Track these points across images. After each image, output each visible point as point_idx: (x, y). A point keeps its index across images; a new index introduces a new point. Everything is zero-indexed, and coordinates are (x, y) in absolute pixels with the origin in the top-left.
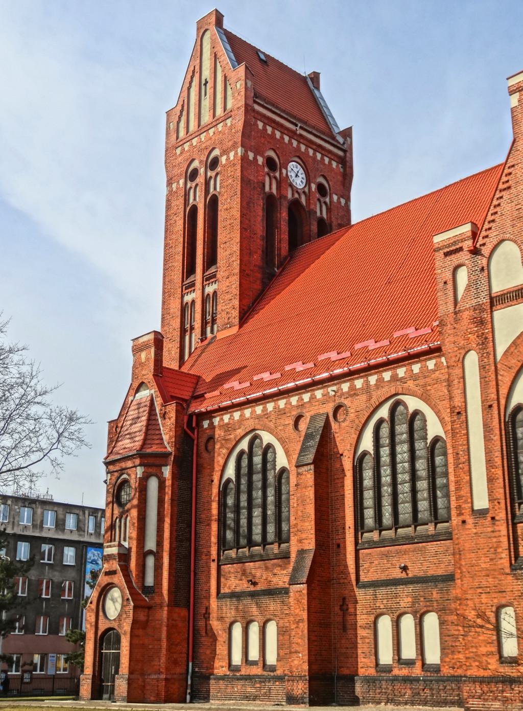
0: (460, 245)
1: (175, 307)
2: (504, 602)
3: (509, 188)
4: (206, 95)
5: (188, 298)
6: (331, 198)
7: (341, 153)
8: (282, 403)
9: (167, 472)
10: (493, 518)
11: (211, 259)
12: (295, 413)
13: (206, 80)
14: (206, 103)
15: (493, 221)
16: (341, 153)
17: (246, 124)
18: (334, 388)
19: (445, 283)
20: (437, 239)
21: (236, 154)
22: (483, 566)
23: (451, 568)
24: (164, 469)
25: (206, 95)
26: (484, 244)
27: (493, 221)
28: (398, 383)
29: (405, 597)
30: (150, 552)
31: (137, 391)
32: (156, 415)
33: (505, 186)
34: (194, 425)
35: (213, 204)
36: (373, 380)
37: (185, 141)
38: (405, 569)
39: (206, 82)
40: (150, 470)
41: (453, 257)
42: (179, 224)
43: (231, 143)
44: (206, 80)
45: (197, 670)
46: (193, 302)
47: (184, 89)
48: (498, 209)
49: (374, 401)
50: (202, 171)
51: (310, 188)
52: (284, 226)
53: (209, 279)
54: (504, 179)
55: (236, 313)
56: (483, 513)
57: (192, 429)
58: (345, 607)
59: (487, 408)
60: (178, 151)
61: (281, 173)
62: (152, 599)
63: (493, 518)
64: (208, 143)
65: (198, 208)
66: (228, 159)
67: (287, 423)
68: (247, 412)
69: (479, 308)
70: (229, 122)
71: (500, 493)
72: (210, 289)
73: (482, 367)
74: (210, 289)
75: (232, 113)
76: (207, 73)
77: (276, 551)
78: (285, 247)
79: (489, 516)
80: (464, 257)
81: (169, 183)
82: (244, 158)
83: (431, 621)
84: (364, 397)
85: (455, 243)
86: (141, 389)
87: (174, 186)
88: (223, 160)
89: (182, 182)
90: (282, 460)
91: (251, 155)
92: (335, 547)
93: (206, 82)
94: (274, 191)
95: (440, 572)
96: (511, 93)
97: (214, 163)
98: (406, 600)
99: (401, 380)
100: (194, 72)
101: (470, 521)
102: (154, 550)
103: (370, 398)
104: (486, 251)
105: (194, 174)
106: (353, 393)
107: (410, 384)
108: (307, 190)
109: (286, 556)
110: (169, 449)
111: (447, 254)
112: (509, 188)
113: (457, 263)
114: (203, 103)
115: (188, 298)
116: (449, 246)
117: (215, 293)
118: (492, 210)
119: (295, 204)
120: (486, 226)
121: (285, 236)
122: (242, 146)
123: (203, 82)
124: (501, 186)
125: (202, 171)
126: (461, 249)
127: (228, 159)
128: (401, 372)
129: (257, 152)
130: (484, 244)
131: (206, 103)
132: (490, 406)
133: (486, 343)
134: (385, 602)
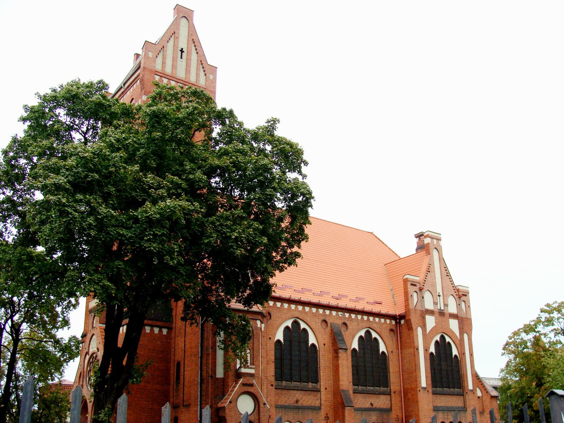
0: (415, 284)
4: (181, 58)
8: (314, 310)
10: (428, 391)
13: (182, 49)
14: (181, 64)
18: (342, 313)
25: (181, 58)
28: (370, 323)
33: (428, 270)
36: (359, 317)
44: (182, 49)
56: (424, 389)
59: (426, 350)
67: (317, 321)
68: (293, 307)
69: (422, 311)
71: (430, 382)
77: (310, 387)
79: (427, 390)
85: (414, 282)
95: (385, 407)
99: (371, 322)
103: (358, 325)
107: (375, 325)
109: (319, 391)
111: (412, 284)
126: (415, 285)
128: (371, 319)
133: (424, 327)
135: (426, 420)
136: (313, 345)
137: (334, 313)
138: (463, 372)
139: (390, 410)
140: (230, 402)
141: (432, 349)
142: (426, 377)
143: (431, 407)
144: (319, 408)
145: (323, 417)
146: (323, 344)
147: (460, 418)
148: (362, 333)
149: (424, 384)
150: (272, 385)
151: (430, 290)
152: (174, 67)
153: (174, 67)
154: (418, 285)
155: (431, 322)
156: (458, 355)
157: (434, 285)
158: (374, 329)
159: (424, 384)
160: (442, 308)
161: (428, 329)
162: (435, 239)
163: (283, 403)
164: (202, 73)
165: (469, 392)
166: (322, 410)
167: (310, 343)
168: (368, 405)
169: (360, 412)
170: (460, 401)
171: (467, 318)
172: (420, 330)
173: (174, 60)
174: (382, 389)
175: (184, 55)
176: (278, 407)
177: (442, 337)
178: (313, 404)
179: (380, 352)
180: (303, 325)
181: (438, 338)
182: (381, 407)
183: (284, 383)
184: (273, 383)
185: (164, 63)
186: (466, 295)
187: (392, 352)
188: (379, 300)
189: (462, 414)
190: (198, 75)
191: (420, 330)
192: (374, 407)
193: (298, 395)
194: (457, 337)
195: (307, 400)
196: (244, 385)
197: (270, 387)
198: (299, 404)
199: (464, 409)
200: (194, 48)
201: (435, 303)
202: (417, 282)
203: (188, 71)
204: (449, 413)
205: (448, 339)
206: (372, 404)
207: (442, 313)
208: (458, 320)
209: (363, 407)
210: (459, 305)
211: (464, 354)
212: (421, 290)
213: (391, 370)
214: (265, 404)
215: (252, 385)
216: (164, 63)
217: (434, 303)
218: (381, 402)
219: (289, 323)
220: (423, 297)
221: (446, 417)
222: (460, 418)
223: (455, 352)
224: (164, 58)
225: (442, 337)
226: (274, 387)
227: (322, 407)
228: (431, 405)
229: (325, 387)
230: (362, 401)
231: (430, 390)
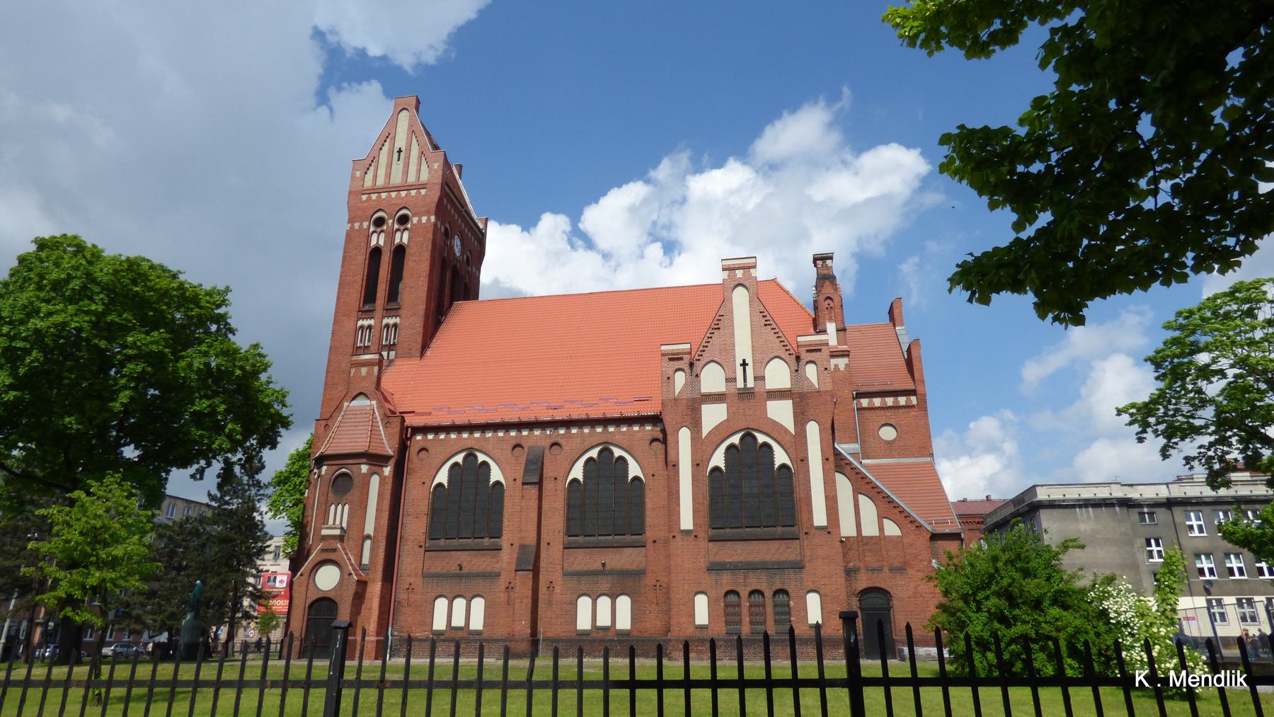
1: (349, 325)
2: (701, 590)
3: (719, 328)
4: (399, 160)
5: (366, 323)
6: (472, 269)
7: (481, 236)
9: (387, 471)
10: (696, 536)
11: (393, 295)
12: (514, 442)
14: (398, 168)
15: (706, 346)
16: (481, 236)
17: (440, 199)
19: (668, 378)
20: (663, 348)
21: (429, 219)
22: (687, 566)
23: (642, 566)
24: (384, 469)
25: (399, 160)
26: (699, 360)
27: (706, 346)
29: (605, 584)
30: (368, 537)
31: (354, 399)
32: (377, 422)
33: (716, 327)
34: (409, 436)
35: (400, 251)
37: (373, 191)
38: (604, 565)
39: (400, 151)
40: (373, 468)
41: (675, 362)
42: (360, 261)
43: (424, 209)
45: (395, 633)
46: (370, 327)
47: (375, 148)
48: (709, 340)
49: (587, 445)
50: (390, 221)
51: (463, 258)
52: (448, 283)
53: (392, 310)
54: (716, 322)
55: (419, 347)
56: (688, 532)
57: (408, 439)
58: (551, 588)
59: (697, 465)
60: (364, 197)
61: (451, 243)
62: (367, 574)
63: (696, 536)
64: (400, 201)
65: (383, 252)
66: (420, 221)
67: (504, 447)
70: (423, 192)
72: (391, 321)
73: (693, 439)
74: (391, 321)
75: (428, 186)
76: (401, 142)
77: (487, 544)
78: (447, 299)
80: (684, 364)
81: (351, 220)
82: (435, 225)
83: (624, 603)
84: (579, 441)
85: (678, 354)
86: (358, 398)
87: (357, 225)
88: (415, 220)
89: (365, 224)
90: (496, 475)
91: (439, 223)
92: (546, 544)
93: (400, 151)
94: (445, 255)
95: (633, 567)
96: (724, 269)
97: (404, 220)
98: (605, 585)
100: (388, 136)
101: (679, 536)
102: (372, 534)
104: (698, 365)
105: (380, 222)
106: (568, 434)
108: (461, 258)
110: (391, 453)
111: (670, 359)
112: (719, 328)
113: (678, 367)
114: (394, 166)
115: (366, 323)
116: (675, 354)
117: (395, 325)
118: (706, 339)
119: (455, 267)
120: (701, 348)
121: (447, 291)
122: (435, 215)
123: (396, 150)
124: (713, 326)
125: (390, 221)
126: (681, 359)
127: (420, 221)
128: (611, 429)
129: (443, 223)
130: (699, 360)
131: (398, 168)
132: (698, 465)
133: (696, 425)
134: (588, 586)
135: (686, 588)
136: (498, 483)
137: (537, 432)
138: (799, 492)
139: (638, 574)
140: (301, 575)
141: (718, 460)
142: (695, 512)
143: (703, 563)
144: (498, 575)
145: (503, 587)
146: (512, 480)
147: (783, 583)
148: (594, 453)
149: (687, 522)
150: (421, 546)
151: (715, 359)
152: (388, 175)
153: (388, 175)
154: (684, 356)
155: (713, 415)
156: (789, 463)
157: (730, 348)
158: (616, 443)
159: (687, 522)
160: (750, 384)
161: (705, 430)
162: (739, 268)
163: (438, 570)
164: (424, 166)
165: (812, 532)
166: (502, 577)
167: (493, 480)
168: (598, 566)
169: (575, 578)
170: (789, 550)
171: (819, 392)
172: (685, 436)
173: (389, 166)
174: (628, 538)
175: (402, 155)
176: (427, 576)
177: (748, 437)
178: (489, 569)
179: (630, 479)
180: (481, 457)
181: (736, 439)
182: (626, 567)
183: (442, 542)
184: (423, 544)
185: (375, 176)
186: (819, 350)
187: (653, 475)
188: (644, 395)
189: (791, 574)
190: (419, 171)
191: (685, 436)
192: (608, 567)
193: (464, 557)
194: (787, 431)
195: (474, 563)
196: (323, 550)
197: (419, 550)
198: (465, 571)
199: (798, 566)
200: (414, 140)
201: (731, 380)
202: (683, 354)
203: (406, 172)
204: (751, 574)
205: (761, 438)
206: (604, 565)
207: (746, 394)
208: (792, 399)
209: (585, 569)
210: (797, 372)
211: (804, 460)
212: (691, 365)
213: (649, 505)
214: (350, 574)
215: (334, 550)
216: (375, 176)
217: (727, 380)
218: (626, 559)
219: (459, 458)
220: (697, 376)
221: (742, 581)
222: (783, 583)
223: (780, 457)
224: (376, 170)
225: (748, 437)
226: (423, 549)
227: (503, 573)
228: (702, 560)
229: (511, 542)
230: (584, 560)
231: (701, 535)
